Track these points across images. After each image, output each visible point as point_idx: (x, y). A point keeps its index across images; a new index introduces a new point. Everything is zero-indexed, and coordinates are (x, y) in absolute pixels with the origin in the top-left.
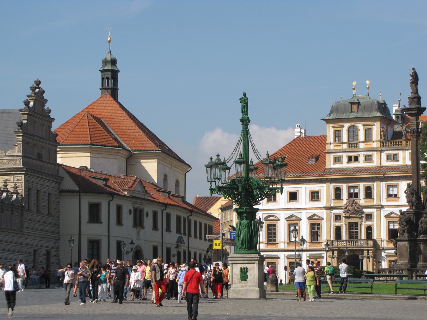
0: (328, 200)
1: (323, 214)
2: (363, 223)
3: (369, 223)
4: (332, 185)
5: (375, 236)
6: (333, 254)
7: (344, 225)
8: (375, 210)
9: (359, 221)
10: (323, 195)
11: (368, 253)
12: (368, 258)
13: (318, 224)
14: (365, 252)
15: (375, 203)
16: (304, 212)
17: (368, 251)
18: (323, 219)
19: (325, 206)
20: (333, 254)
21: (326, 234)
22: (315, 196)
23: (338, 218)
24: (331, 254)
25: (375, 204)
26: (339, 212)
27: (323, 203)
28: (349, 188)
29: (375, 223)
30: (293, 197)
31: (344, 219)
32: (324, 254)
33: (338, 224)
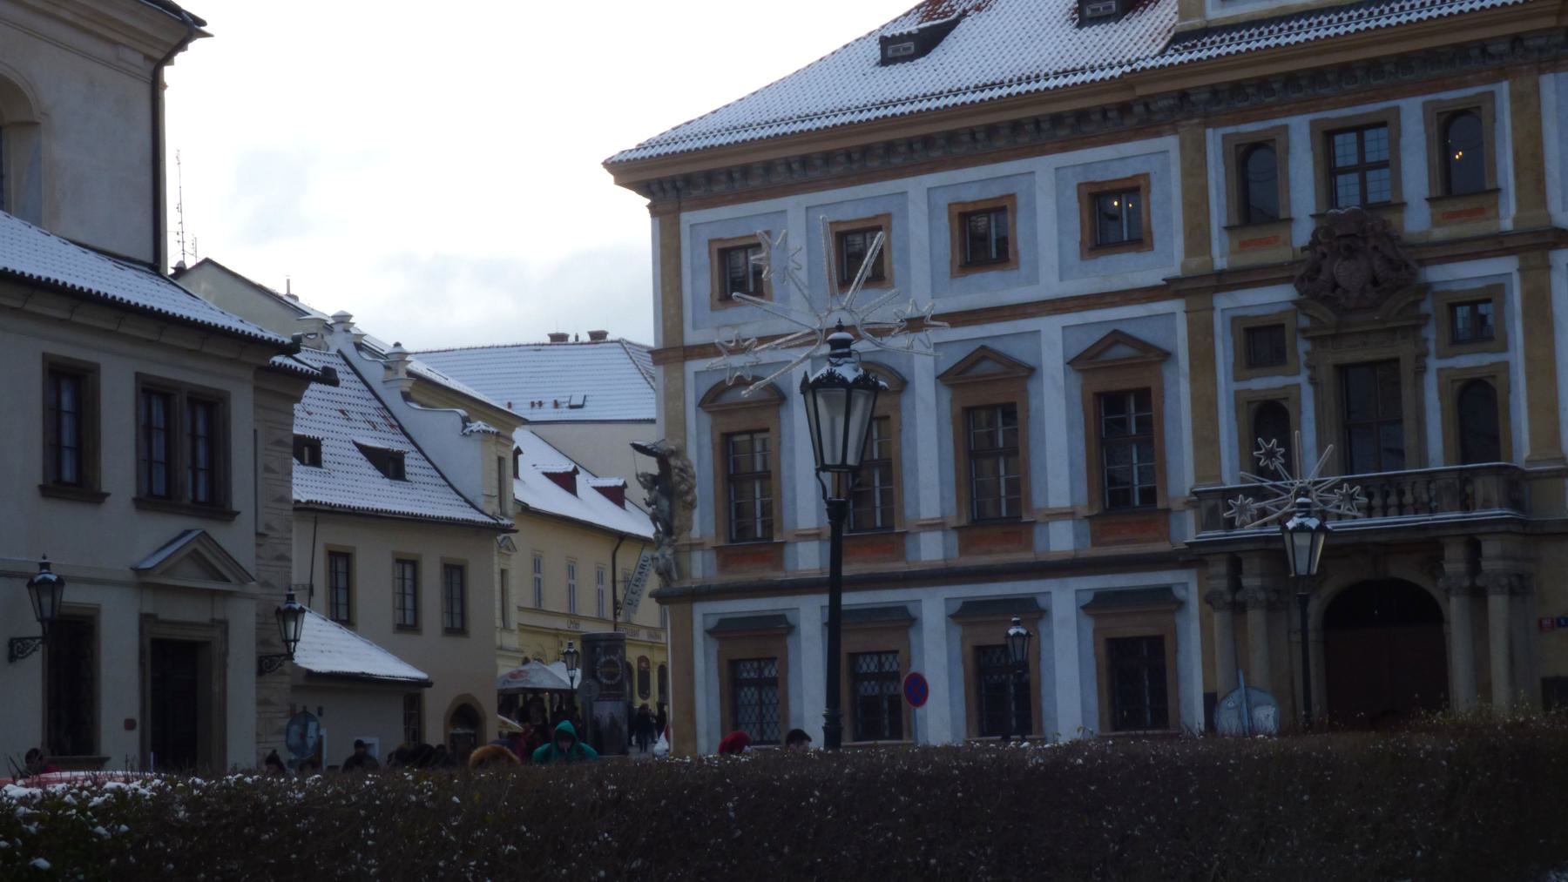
0: (1197, 238)
1: (1169, 324)
2: (1434, 364)
3: (1470, 361)
4: (1214, 139)
5: (1523, 446)
6: (1236, 585)
7: (1299, 385)
8: (1505, 266)
9: (1404, 350)
10: (1167, 209)
11: (1474, 567)
12: (1478, 596)
13: (1144, 397)
14: (1454, 561)
15: (1507, 217)
16: (1051, 328)
17: (1474, 547)
18: (1166, 356)
19: (1175, 270)
20: (1236, 585)
21: (1195, 447)
22: (1110, 219)
23: (1261, 343)
24: (1221, 584)
25: (1507, 224)
26: (1274, 298)
27: (1167, 258)
28: (1326, 137)
29: (1517, 356)
30: (982, 239)
31: (1303, 347)
32: (1187, 584)
33: (1265, 383)
